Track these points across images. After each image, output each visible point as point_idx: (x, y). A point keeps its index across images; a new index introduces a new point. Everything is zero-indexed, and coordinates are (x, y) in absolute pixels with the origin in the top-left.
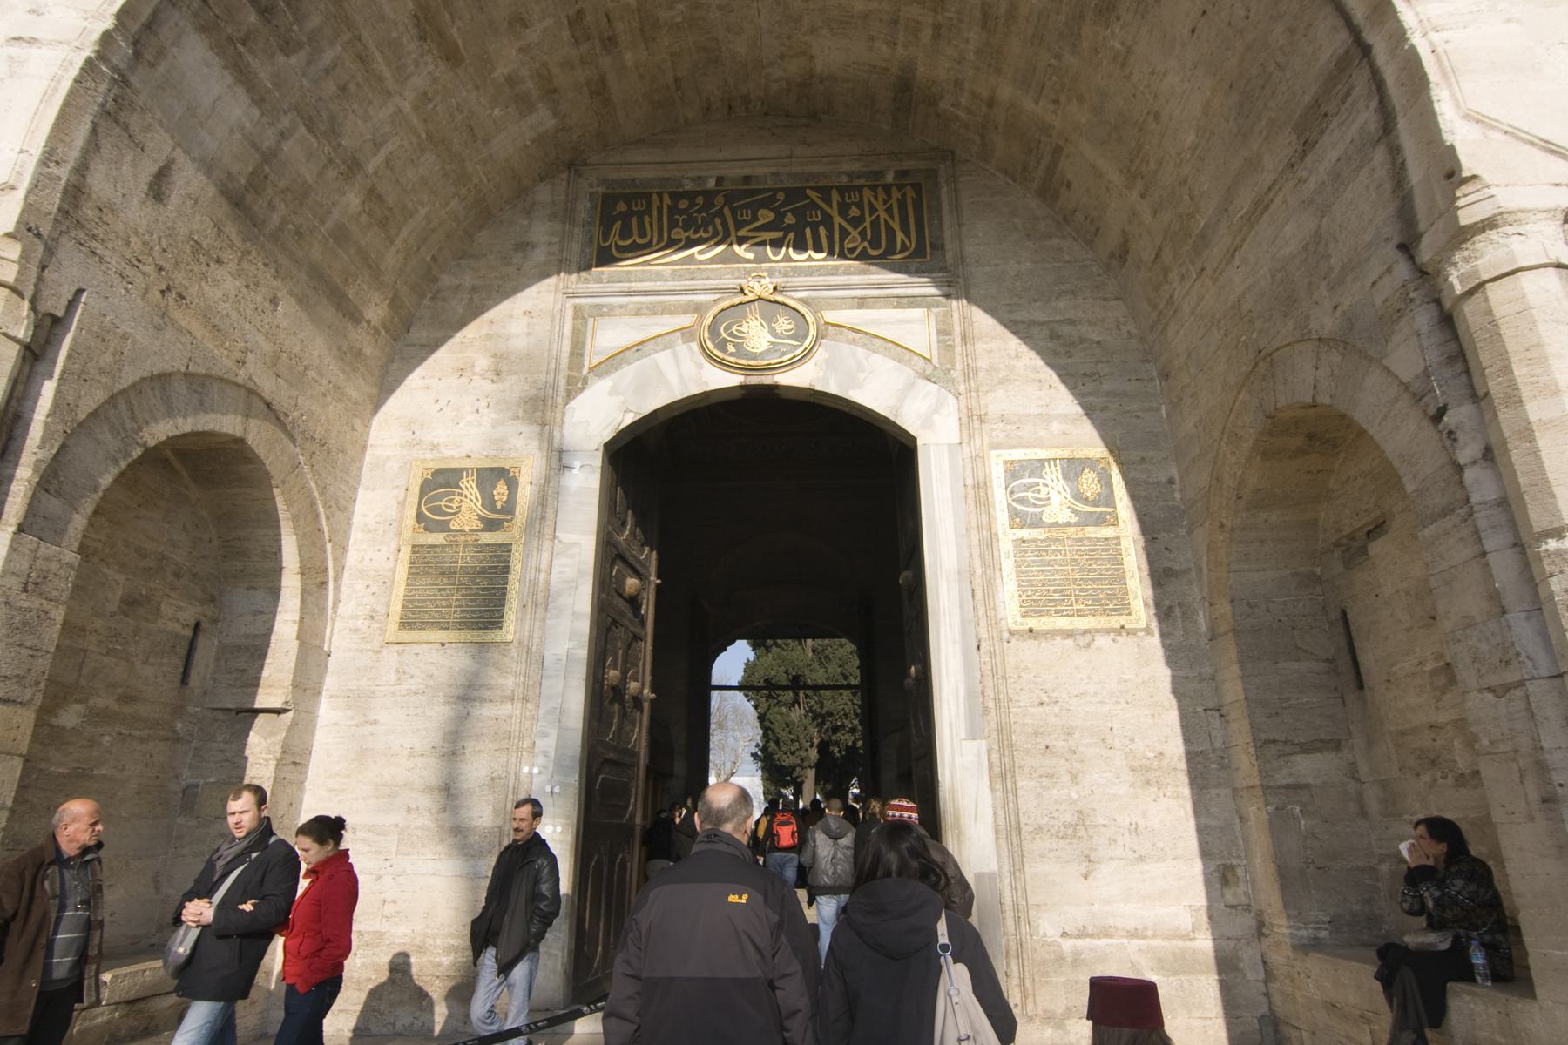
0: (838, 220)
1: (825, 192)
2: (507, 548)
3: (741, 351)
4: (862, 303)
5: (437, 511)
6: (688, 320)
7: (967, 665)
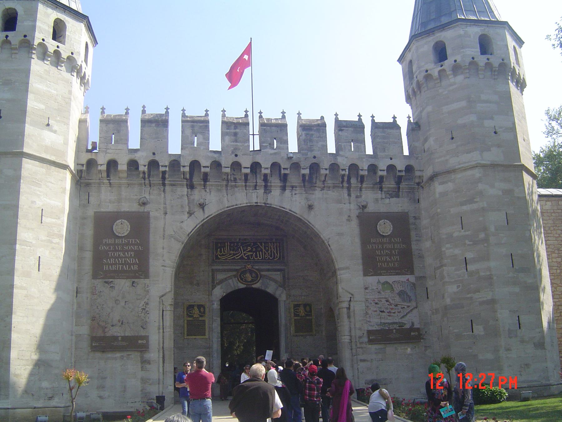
0: (264, 250)
1: (261, 243)
2: (204, 321)
3: (246, 281)
4: (268, 270)
5: (190, 313)
6: (235, 273)
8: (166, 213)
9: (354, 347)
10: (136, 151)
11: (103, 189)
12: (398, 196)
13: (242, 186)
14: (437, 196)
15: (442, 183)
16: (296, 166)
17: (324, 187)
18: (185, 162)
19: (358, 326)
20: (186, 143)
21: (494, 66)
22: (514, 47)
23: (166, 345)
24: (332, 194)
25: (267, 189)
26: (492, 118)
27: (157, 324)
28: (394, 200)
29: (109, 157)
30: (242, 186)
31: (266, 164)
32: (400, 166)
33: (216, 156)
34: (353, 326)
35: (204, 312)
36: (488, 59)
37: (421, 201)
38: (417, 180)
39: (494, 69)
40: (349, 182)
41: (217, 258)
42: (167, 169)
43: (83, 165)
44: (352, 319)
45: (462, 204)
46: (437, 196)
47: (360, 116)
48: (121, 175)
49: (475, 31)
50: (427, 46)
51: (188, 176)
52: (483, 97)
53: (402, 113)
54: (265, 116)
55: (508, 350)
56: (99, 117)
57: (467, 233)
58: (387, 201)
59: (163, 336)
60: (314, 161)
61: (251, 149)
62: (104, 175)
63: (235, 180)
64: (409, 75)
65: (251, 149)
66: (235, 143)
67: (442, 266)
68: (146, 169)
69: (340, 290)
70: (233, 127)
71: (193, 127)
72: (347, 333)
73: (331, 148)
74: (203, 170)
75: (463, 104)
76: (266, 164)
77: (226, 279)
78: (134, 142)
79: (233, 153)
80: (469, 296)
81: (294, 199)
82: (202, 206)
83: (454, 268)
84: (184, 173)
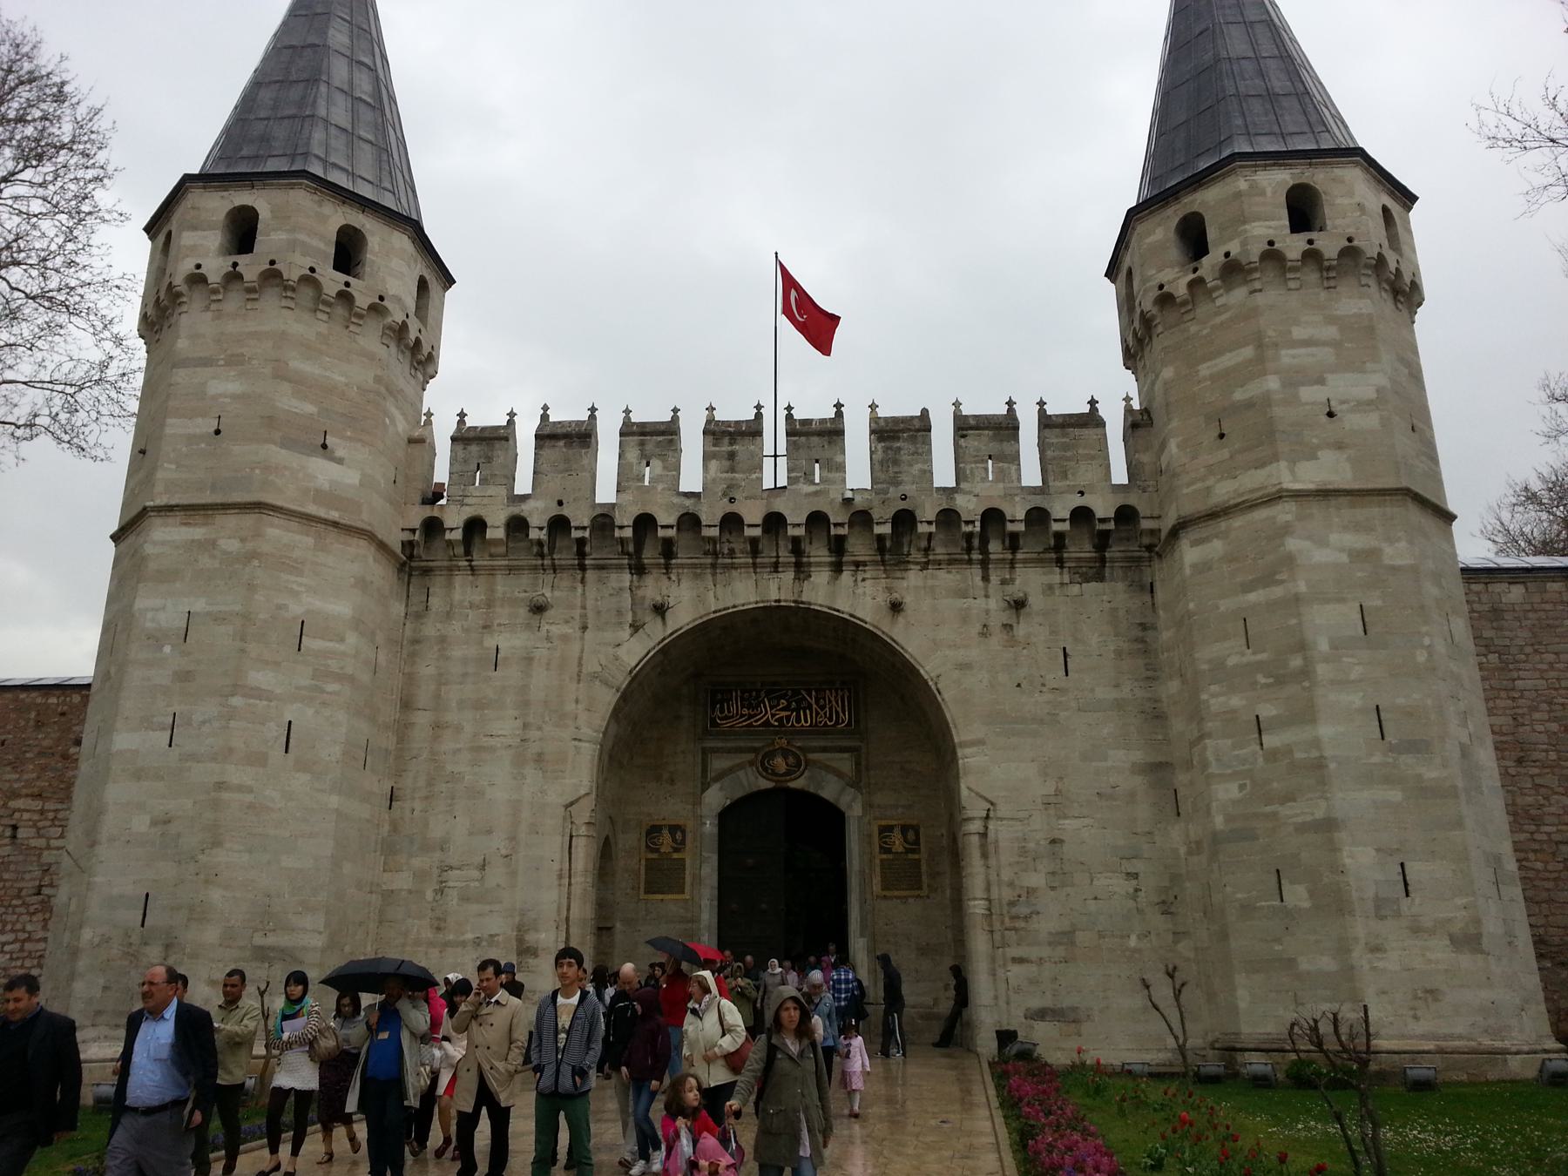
3: (774, 773)
4: (824, 750)
6: (752, 756)
7: (861, 908)
8: (584, 628)
9: (997, 926)
10: (524, 498)
11: (458, 580)
12: (1100, 577)
13: (746, 566)
14: (1188, 571)
15: (1196, 543)
16: (862, 519)
17: (927, 563)
18: (625, 518)
19: (1006, 875)
20: (626, 479)
21: (1326, 256)
22: (1385, 210)
23: (575, 913)
24: (946, 578)
25: (802, 570)
26: (1321, 381)
27: (556, 866)
28: (1093, 584)
29: (468, 512)
30: (746, 566)
31: (796, 516)
32: (1103, 508)
33: (688, 502)
34: (993, 877)
35: (683, 842)
36: (1310, 242)
37: (1157, 585)
38: (1146, 540)
39: (1326, 264)
40: (984, 550)
41: (714, 724)
42: (587, 534)
43: (413, 531)
44: (992, 862)
45: (1248, 587)
46: (1188, 571)
47: (1010, 403)
48: (493, 550)
49: (1277, 180)
50: (1161, 231)
51: (631, 548)
52: (1298, 333)
53: (1113, 389)
54: (797, 415)
55: (1376, 949)
56: (451, 428)
57: (1259, 657)
58: (1075, 589)
59: (569, 894)
60: (903, 505)
61: (768, 483)
62: (460, 550)
63: (732, 553)
64: (1127, 304)
65: (768, 483)
66: (730, 475)
67: (1201, 738)
68: (543, 535)
69: (964, 792)
70: (726, 440)
71: (642, 444)
72: (979, 893)
73: (944, 476)
74: (661, 533)
75: (1248, 352)
76: (796, 516)
77: (731, 770)
78: (523, 483)
79: (724, 495)
80: (1268, 809)
81: (860, 591)
82: (660, 610)
83: (1229, 742)
84: (622, 541)
